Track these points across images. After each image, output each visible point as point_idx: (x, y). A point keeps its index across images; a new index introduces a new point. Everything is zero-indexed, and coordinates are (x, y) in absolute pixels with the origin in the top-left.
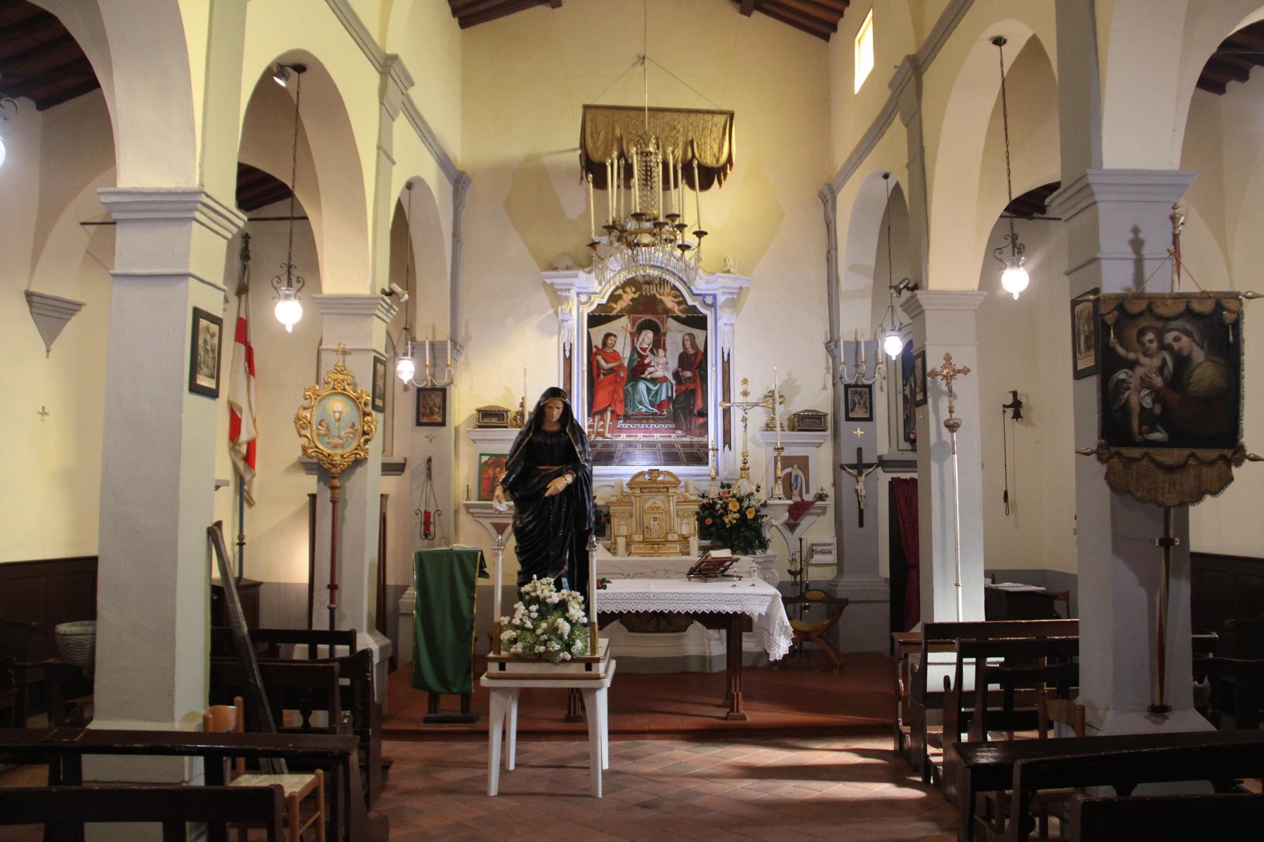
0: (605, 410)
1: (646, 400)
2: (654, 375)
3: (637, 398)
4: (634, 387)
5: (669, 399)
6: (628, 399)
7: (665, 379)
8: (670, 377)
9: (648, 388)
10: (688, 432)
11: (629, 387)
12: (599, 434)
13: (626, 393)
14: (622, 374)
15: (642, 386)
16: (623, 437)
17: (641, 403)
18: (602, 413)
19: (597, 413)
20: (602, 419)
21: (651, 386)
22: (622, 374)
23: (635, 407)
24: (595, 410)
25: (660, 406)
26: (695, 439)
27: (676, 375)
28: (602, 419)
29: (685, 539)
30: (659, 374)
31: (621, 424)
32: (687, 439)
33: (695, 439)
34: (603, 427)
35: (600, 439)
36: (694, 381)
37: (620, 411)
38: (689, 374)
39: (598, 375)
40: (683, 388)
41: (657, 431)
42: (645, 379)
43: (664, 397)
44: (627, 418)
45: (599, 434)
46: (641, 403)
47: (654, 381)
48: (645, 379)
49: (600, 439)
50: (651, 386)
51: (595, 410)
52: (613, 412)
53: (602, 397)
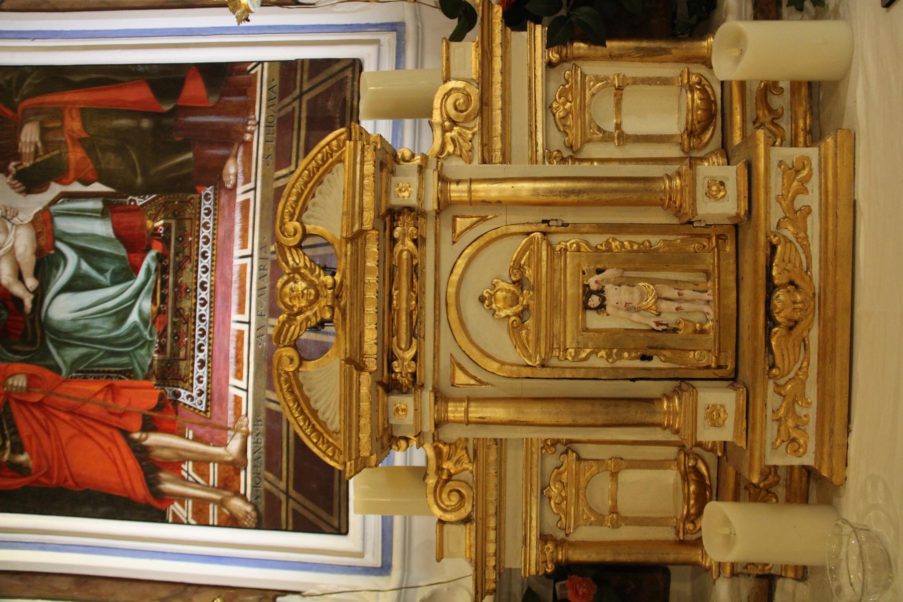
0: (142, 452)
1: (110, 295)
2: (27, 260)
3: (102, 328)
4: (65, 337)
5: (110, 207)
6: (107, 362)
7: (43, 224)
8: (36, 203)
9: (71, 287)
10: (231, 139)
11: (65, 357)
12: (228, 483)
13: (86, 370)
14: (20, 381)
15: (63, 309)
16: (241, 388)
17: (121, 315)
18: (151, 466)
19: (152, 483)
20: (174, 466)
21: (63, 277)
22: (20, 381)
23: (134, 340)
24: (140, 491)
25: (134, 242)
26: (261, 111)
27: (31, 181)
28: (174, 466)
29: (711, 120)
30: (23, 243)
31: (191, 397)
32: (259, 140)
33: (261, 111)
34: (201, 464)
35: (246, 480)
36: (58, 113)
37: (143, 396)
38: (30, 135)
39: (20, 470)
40: (75, 155)
41: (222, 255)
42: (39, 295)
43: (103, 228)
44: (170, 373)
45: (228, 483)
46: (121, 315)
47: (46, 263)
48: (39, 295)
49: (246, 480)
50: (63, 277)
51: (140, 491)
52: (150, 426)
53: (96, 460)
